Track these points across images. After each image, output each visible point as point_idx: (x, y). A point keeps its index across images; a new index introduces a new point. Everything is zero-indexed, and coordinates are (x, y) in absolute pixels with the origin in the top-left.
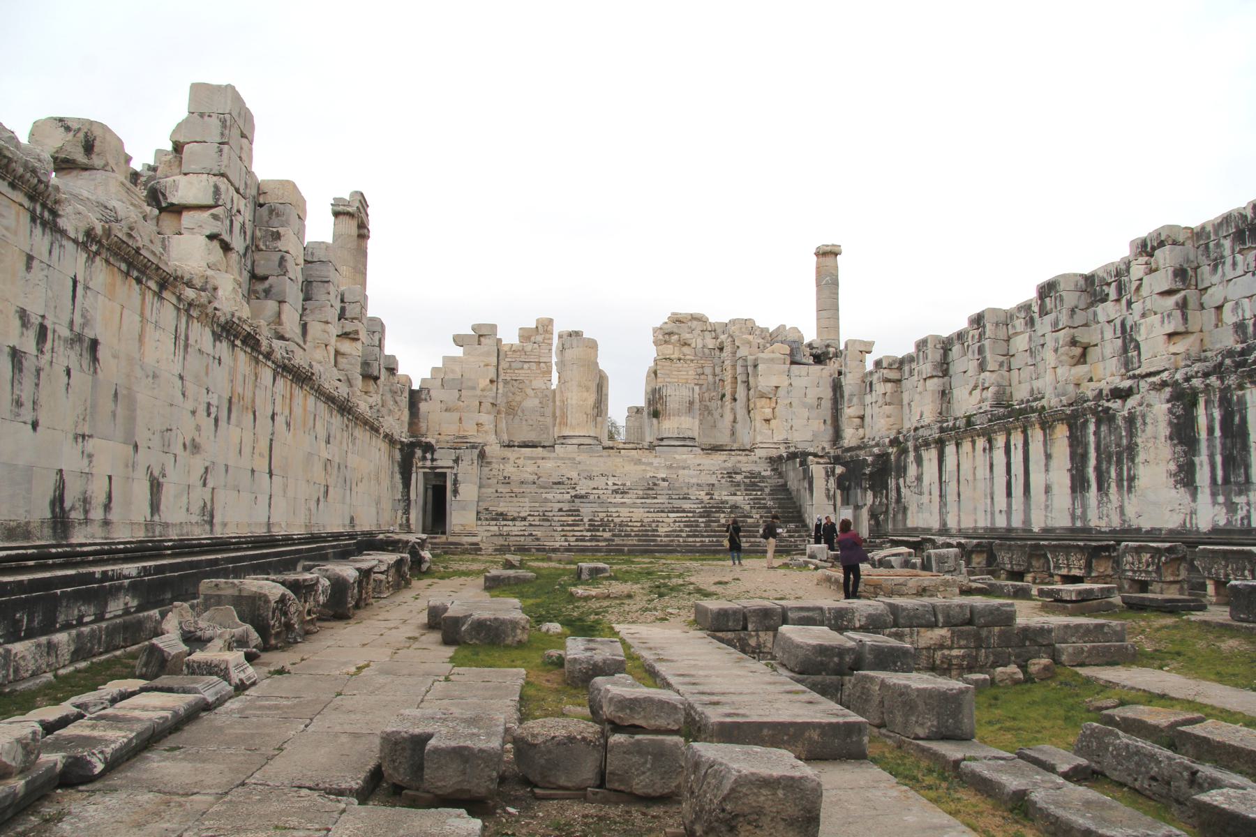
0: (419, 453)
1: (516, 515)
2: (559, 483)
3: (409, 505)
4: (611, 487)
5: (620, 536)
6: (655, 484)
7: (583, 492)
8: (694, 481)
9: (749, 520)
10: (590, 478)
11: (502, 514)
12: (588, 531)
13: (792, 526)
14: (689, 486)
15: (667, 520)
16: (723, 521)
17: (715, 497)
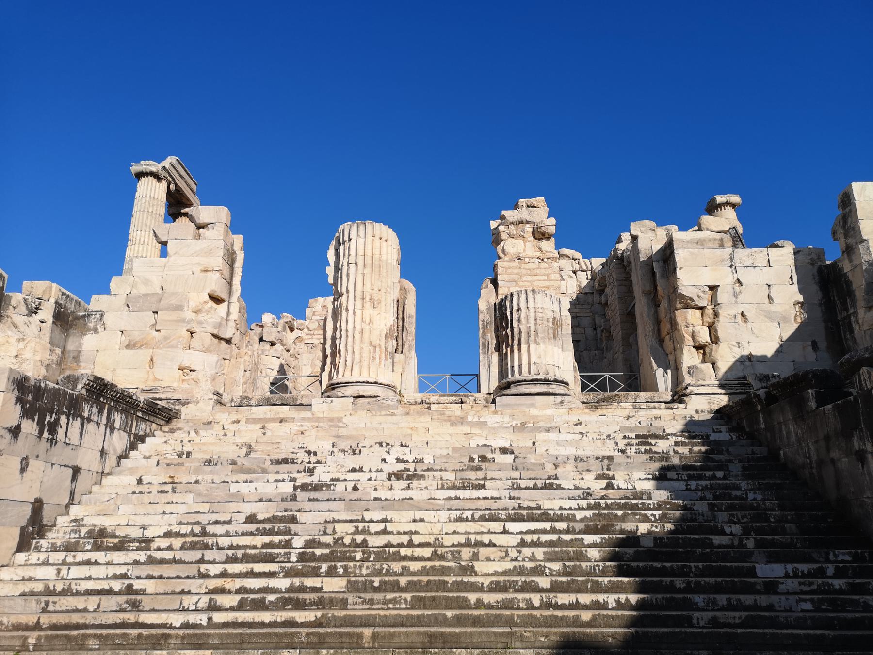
1: (136, 533)
2: (285, 461)
4: (393, 466)
5: (367, 587)
6: (484, 459)
7: (326, 478)
8: (563, 451)
9: (717, 540)
12: (289, 574)
13: (844, 555)
15: (499, 540)
17: (619, 481)
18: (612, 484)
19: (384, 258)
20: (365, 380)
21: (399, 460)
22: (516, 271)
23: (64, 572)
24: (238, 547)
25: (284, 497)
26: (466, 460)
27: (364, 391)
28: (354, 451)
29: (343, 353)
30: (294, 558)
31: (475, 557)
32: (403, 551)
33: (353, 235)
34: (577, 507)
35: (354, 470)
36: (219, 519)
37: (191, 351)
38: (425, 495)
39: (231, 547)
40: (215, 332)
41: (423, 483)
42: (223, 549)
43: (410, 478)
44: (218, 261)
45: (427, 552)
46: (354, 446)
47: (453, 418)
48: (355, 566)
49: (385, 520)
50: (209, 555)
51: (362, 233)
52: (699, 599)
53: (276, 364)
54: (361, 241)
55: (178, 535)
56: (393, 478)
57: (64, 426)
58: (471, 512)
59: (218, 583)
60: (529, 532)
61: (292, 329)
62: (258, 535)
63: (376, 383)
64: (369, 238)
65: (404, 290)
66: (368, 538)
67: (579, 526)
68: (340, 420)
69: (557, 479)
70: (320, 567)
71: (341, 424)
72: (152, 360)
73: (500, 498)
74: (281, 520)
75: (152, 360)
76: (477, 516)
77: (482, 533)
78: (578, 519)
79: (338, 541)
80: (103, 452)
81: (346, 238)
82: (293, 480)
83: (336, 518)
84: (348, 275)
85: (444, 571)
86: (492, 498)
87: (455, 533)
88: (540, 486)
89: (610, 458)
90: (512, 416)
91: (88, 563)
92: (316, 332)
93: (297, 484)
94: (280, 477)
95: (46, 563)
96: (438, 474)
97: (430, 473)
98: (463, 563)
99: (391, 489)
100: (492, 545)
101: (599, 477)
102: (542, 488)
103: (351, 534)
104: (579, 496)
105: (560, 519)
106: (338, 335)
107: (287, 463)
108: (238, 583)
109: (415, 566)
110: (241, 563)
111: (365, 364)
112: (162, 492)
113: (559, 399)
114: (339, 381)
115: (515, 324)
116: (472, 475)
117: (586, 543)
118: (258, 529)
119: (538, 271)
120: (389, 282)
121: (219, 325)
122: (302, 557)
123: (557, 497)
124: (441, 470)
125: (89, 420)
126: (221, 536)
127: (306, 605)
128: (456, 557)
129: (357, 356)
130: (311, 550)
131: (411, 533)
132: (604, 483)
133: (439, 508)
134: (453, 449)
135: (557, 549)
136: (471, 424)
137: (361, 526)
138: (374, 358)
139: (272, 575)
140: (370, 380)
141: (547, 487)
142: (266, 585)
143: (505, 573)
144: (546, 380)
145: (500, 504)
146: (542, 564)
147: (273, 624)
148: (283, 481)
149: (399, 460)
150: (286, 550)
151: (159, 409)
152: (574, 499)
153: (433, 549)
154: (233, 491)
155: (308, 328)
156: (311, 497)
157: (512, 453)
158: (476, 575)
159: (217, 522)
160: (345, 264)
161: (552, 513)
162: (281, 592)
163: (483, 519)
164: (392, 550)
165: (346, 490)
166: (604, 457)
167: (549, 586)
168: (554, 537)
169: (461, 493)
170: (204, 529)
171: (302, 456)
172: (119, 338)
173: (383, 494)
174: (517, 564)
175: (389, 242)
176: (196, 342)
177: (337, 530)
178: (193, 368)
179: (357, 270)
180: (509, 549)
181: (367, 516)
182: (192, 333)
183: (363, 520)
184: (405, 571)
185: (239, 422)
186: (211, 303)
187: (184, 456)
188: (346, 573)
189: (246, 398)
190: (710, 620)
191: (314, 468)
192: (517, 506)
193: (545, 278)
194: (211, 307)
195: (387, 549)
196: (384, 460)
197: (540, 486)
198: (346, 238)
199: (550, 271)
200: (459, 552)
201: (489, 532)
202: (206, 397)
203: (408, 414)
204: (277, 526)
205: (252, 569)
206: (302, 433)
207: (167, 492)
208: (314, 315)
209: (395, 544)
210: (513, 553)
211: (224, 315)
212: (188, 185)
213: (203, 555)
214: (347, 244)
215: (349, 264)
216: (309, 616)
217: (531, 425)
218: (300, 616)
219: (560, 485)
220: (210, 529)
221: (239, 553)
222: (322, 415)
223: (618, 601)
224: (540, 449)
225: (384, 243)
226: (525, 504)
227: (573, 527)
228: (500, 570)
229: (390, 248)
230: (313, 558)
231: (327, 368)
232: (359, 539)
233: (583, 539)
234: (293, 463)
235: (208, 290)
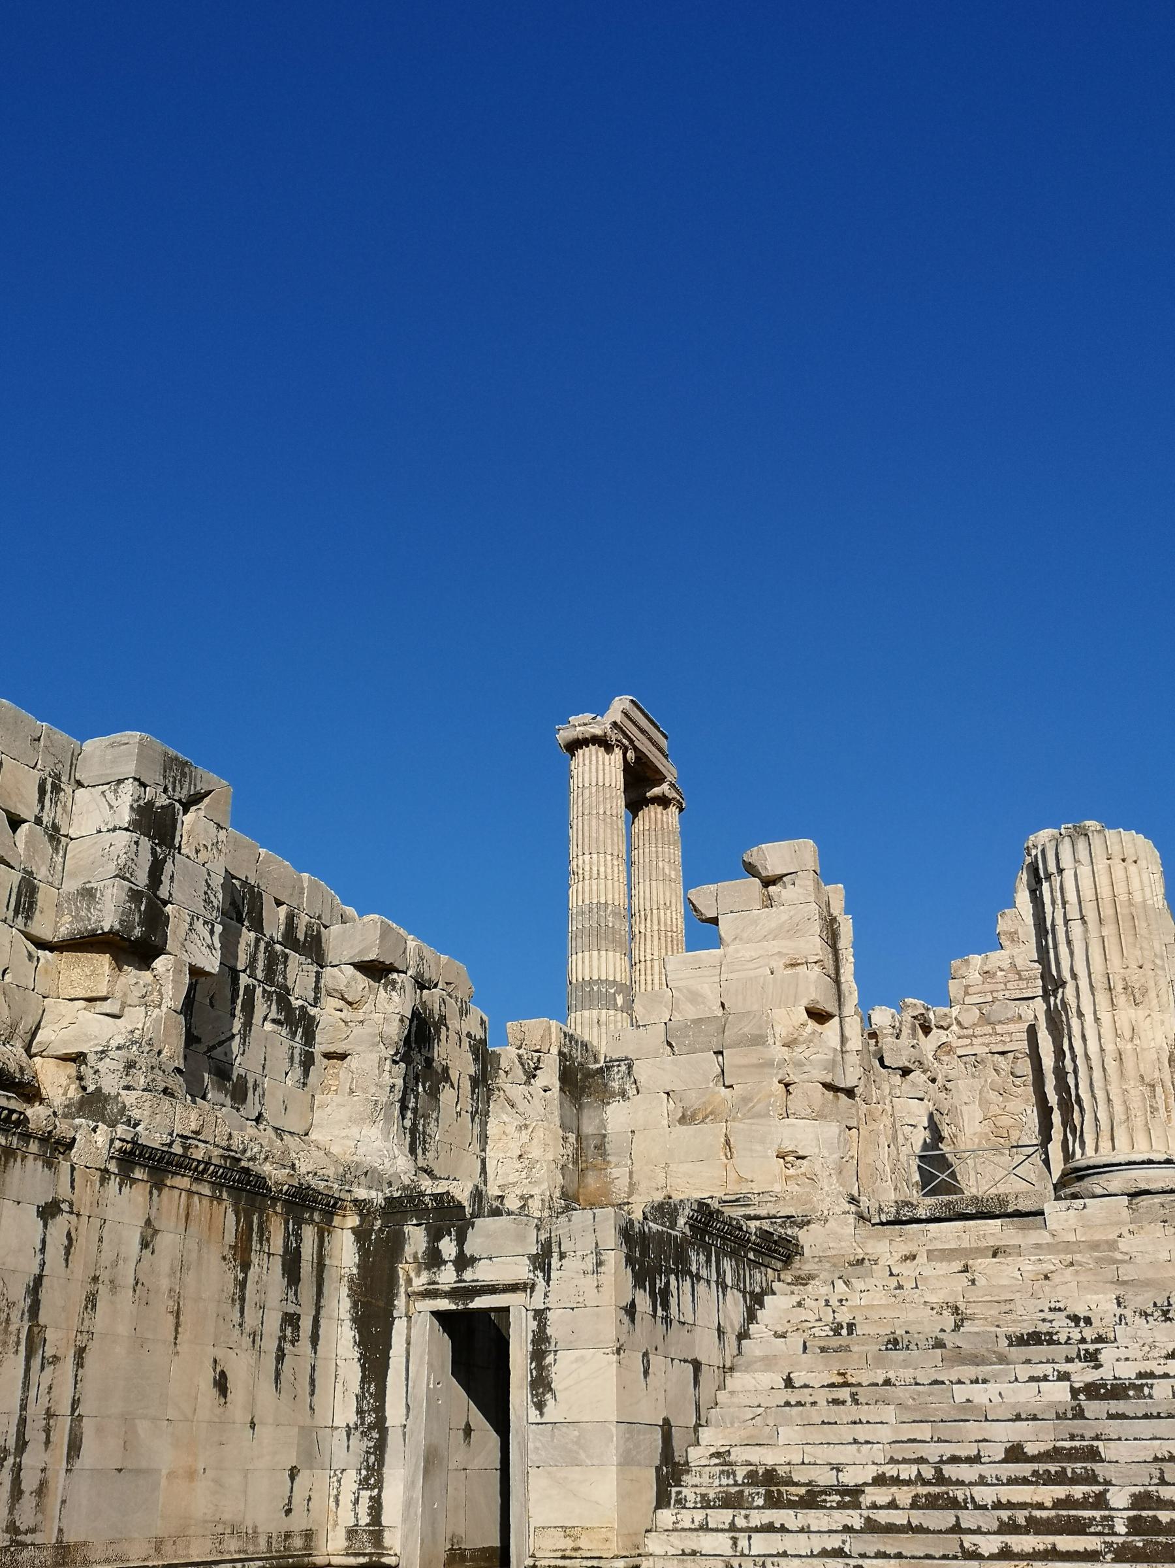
0: (416, 1238)
1: (825, 1478)
2: (1034, 1338)
3: (380, 1448)
7: (1127, 1372)
11: (770, 1478)
19: (1138, 898)
20: (1145, 1157)
23: (743, 1543)
27: (1148, 1180)
29: (1086, 1104)
30: (1121, 1528)
33: (1067, 861)
36: (957, 1453)
37: (791, 1120)
40: (828, 1080)
42: (984, 1507)
44: (813, 945)
51: (1083, 854)
53: (919, 1113)
54: (1084, 871)
55: (896, 1481)
57: (675, 1294)
61: (927, 1030)
62: (1036, 1483)
64: (1101, 865)
68: (1112, 1245)
71: (1119, 1256)
72: (728, 1142)
74: (1072, 1455)
75: (728, 1142)
80: (720, 1332)
81: (1052, 868)
82: (1064, 1377)
84: (1069, 943)
91: (769, 1528)
93: (1077, 1385)
94: (1039, 1370)
95: (704, 1528)
106: (1069, 1067)
107: (1039, 1342)
110: (1028, 1533)
111: (1139, 1122)
112: (836, 1402)
114: (1091, 1162)
118: (1035, 1473)
120: (1157, 945)
121: (831, 1066)
122: (1135, 1525)
125: (699, 1278)
126: (971, 1484)
129: (1118, 1108)
130: (1151, 1513)
138: (1153, 1110)
148: (1045, 1378)
150: (1103, 1513)
151: (775, 1242)
155: (959, 1023)
159: (954, 1460)
160: (1060, 921)
170: (939, 1471)
171: (1061, 1324)
172: (665, 1106)
175: (1142, 863)
176: (797, 1102)
178: (801, 1153)
179: (1086, 931)
182: (787, 1085)
185: (914, 1257)
186: (812, 1025)
187: (844, 1332)
189: (907, 1204)
191: (1097, 1351)
194: (814, 1032)
198: (1052, 868)
202: (838, 1210)
204: (1069, 1468)
206: (1046, 1277)
207: (843, 1403)
208: (967, 994)
211: (835, 1042)
212: (655, 744)
213: (957, 1518)
214: (1056, 880)
215: (1066, 922)
220: (949, 1471)
221: (1021, 1517)
225: (1133, 868)
229: (1145, 876)
230: (1156, 1527)
231: (1057, 1133)
234: (1051, 1342)
235: (804, 1002)
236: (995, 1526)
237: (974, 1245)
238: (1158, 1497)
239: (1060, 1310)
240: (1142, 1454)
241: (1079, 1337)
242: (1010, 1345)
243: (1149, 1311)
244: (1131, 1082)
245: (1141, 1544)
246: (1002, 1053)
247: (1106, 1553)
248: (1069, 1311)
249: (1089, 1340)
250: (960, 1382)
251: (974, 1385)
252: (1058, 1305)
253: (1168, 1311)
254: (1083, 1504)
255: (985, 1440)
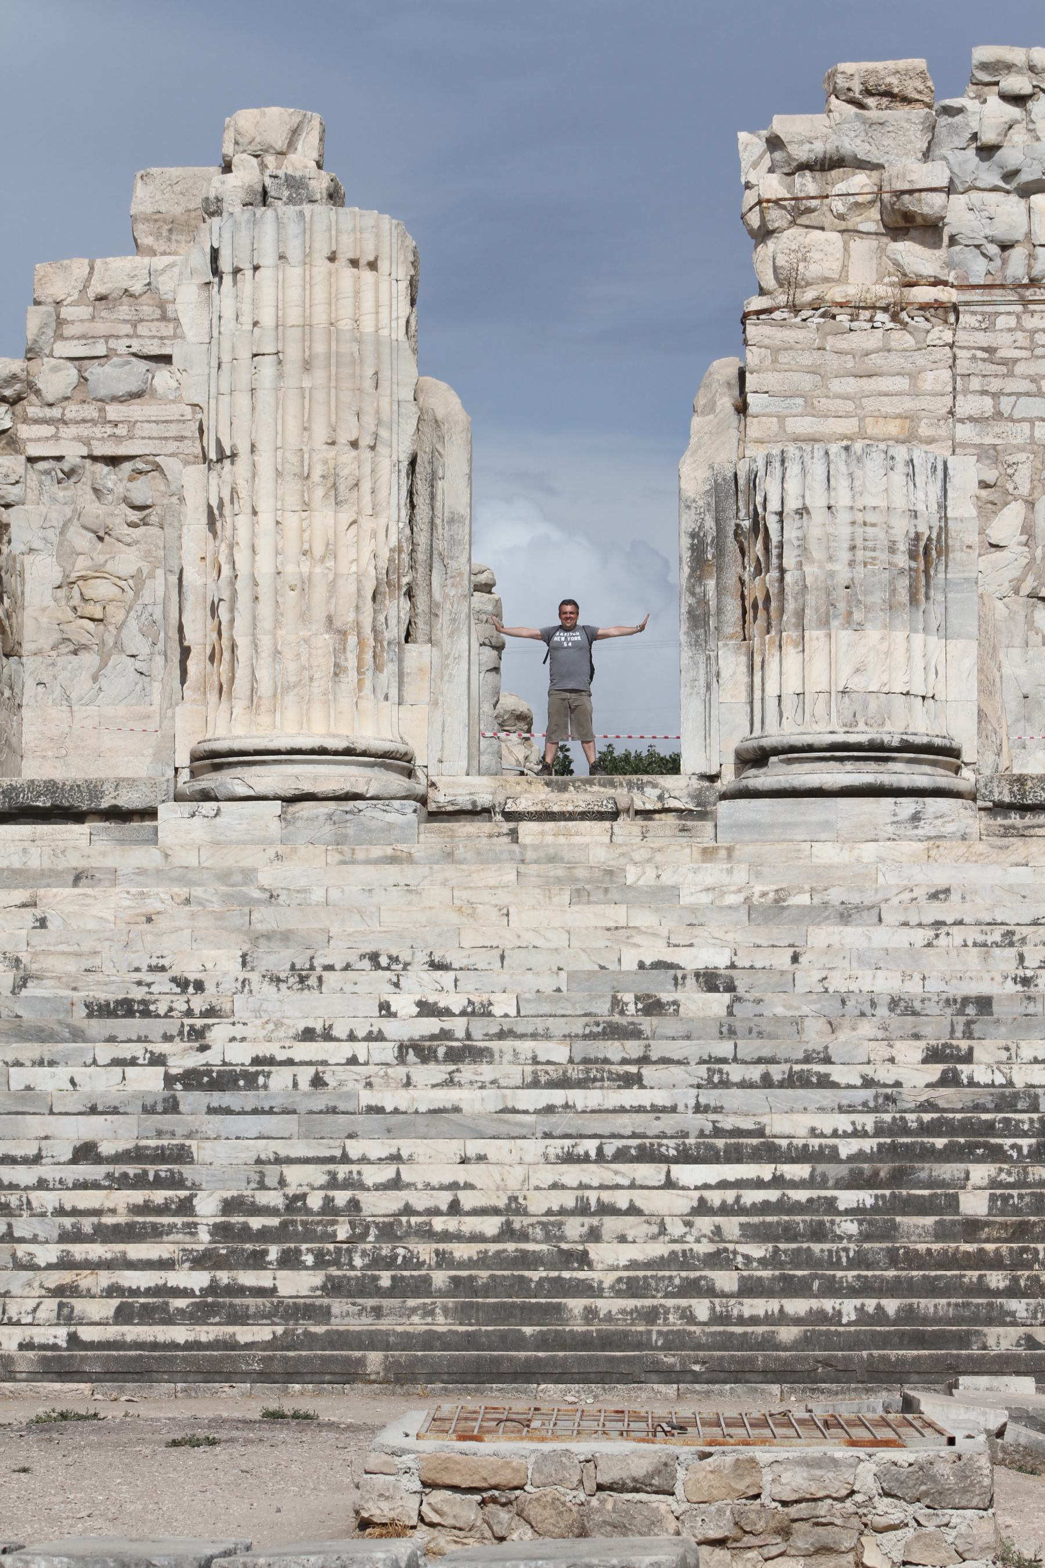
2: (126, 1008)
5: (366, 1288)
7: (240, 1056)
10: (303, 977)
14: (842, 1009)
16: (974, 1204)
18: (955, 1072)
19: (368, 326)
21: (426, 1009)
22: (807, 359)
24: (75, 1212)
25: (149, 1102)
26: (602, 1008)
27: (316, 779)
28: (302, 980)
29: (242, 653)
30: (204, 1236)
31: (594, 1235)
32: (439, 1224)
34: (850, 1129)
35: (308, 1035)
36: (12, 1153)
38: (489, 1101)
39: (60, 1212)
41: (486, 1071)
43: (454, 1056)
45: (491, 1225)
46: (302, 962)
47: (581, 873)
48: (338, 1251)
49: (396, 1158)
50: (22, 1227)
52: (1018, 1306)
56: (411, 1056)
58: (596, 1142)
59: (65, 1277)
60: (723, 1185)
62: (109, 1188)
63: (349, 752)
65: (428, 423)
66: (361, 1196)
67: (840, 1171)
69: (827, 1060)
70: (265, 1253)
71: (256, 894)
73: (674, 1109)
74: (160, 1156)
76: (610, 1150)
77: (618, 1187)
78: (843, 1155)
79: (295, 1203)
82: (157, 1060)
83: (283, 1153)
85: (526, 1260)
86: (655, 1109)
87: (555, 1186)
88: (777, 1077)
89: (984, 1004)
90: (756, 868)
92: (73, 411)
93: (174, 1071)
94: (126, 1051)
96: (526, 1047)
97: (507, 1045)
98: (564, 1246)
99: (408, 1084)
100: (633, 1210)
101: (933, 1056)
102: (781, 1085)
103: (321, 1188)
104: (865, 1104)
105: (803, 1155)
107: (130, 1013)
108: (105, 1279)
109: (462, 1251)
110: (93, 1241)
113: (908, 806)
115: (789, 562)
116: (613, 1049)
117: (841, 1208)
118: (109, 1176)
119: (876, 360)
122: (221, 1231)
123: (812, 1107)
124: (534, 1036)
126: (27, 1188)
127: (248, 1317)
128: (552, 1233)
130: (242, 1219)
131: (454, 1186)
132: (935, 1071)
133: (524, 1132)
134: (572, 976)
135: (769, 1219)
136: (632, 897)
137: (342, 1171)
139: (165, 1265)
140: (332, 744)
141: (793, 1081)
142: (161, 1282)
143: (648, 1265)
144: (875, 746)
145: (668, 1123)
146: (731, 1247)
147: (189, 1346)
148: (133, 1062)
149: (426, 1009)
150: (186, 1219)
152: (850, 1109)
153: (503, 1219)
154: (16, 1085)
156: (215, 1104)
157: (731, 988)
158: (591, 1268)
161: (784, 1143)
162: (194, 1296)
163: (622, 1156)
164: (414, 1220)
165: (295, 1085)
166: (966, 1001)
167: (735, 1288)
168: (773, 1195)
169: (579, 1097)
173: (389, 1099)
174: (677, 1247)
175: (383, 265)
177: (289, 1180)
180: (667, 1220)
181: (355, 1148)
183: (345, 1159)
184: (444, 1260)
188: (321, 1262)
190: (1020, 1338)
191: (208, 1027)
192: (708, 1127)
193: (902, 383)
195: (404, 1219)
196: (385, 1009)
197: (777, 1077)
199: (920, 359)
200: (560, 1225)
201: (633, 1186)
203: (449, 856)
204: (151, 1170)
205: (124, 1253)
206: (149, 920)
209: (420, 1209)
210: (676, 1228)
216: (262, 1333)
217: (804, 899)
218: (245, 1334)
219: (827, 1075)
221: (87, 1224)
222: (192, 860)
223: (860, 1310)
224: (808, 977)
225: (367, 275)
226: (728, 1123)
227: (824, 1176)
228: (640, 1257)
230: (246, 1233)
232: (341, 1198)
233: (835, 1199)
234: (146, 1014)
236: (55, 1234)
237: (47, 864)
238: (253, 1203)
239: (163, 969)
240: (242, 1155)
241: (184, 1007)
242: (90, 1015)
243: (283, 976)
244: (314, 627)
245: (224, 1252)
246: (113, 461)
247: (183, 1262)
248: (173, 972)
249: (197, 1012)
250: (18, 1064)
251: (37, 1069)
252: (161, 962)
253: (307, 977)
254: (163, 1210)
255: (46, 1138)
